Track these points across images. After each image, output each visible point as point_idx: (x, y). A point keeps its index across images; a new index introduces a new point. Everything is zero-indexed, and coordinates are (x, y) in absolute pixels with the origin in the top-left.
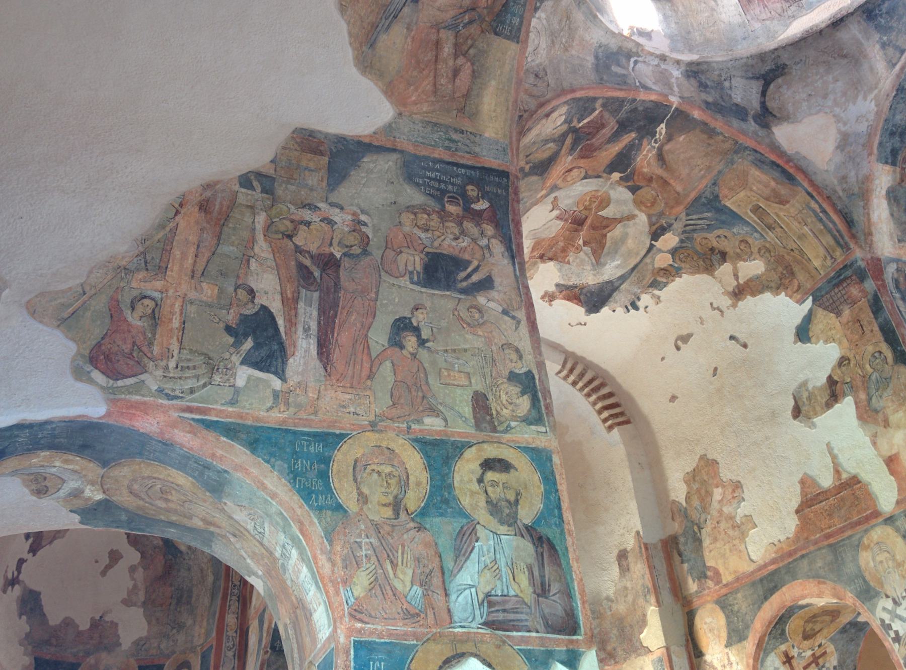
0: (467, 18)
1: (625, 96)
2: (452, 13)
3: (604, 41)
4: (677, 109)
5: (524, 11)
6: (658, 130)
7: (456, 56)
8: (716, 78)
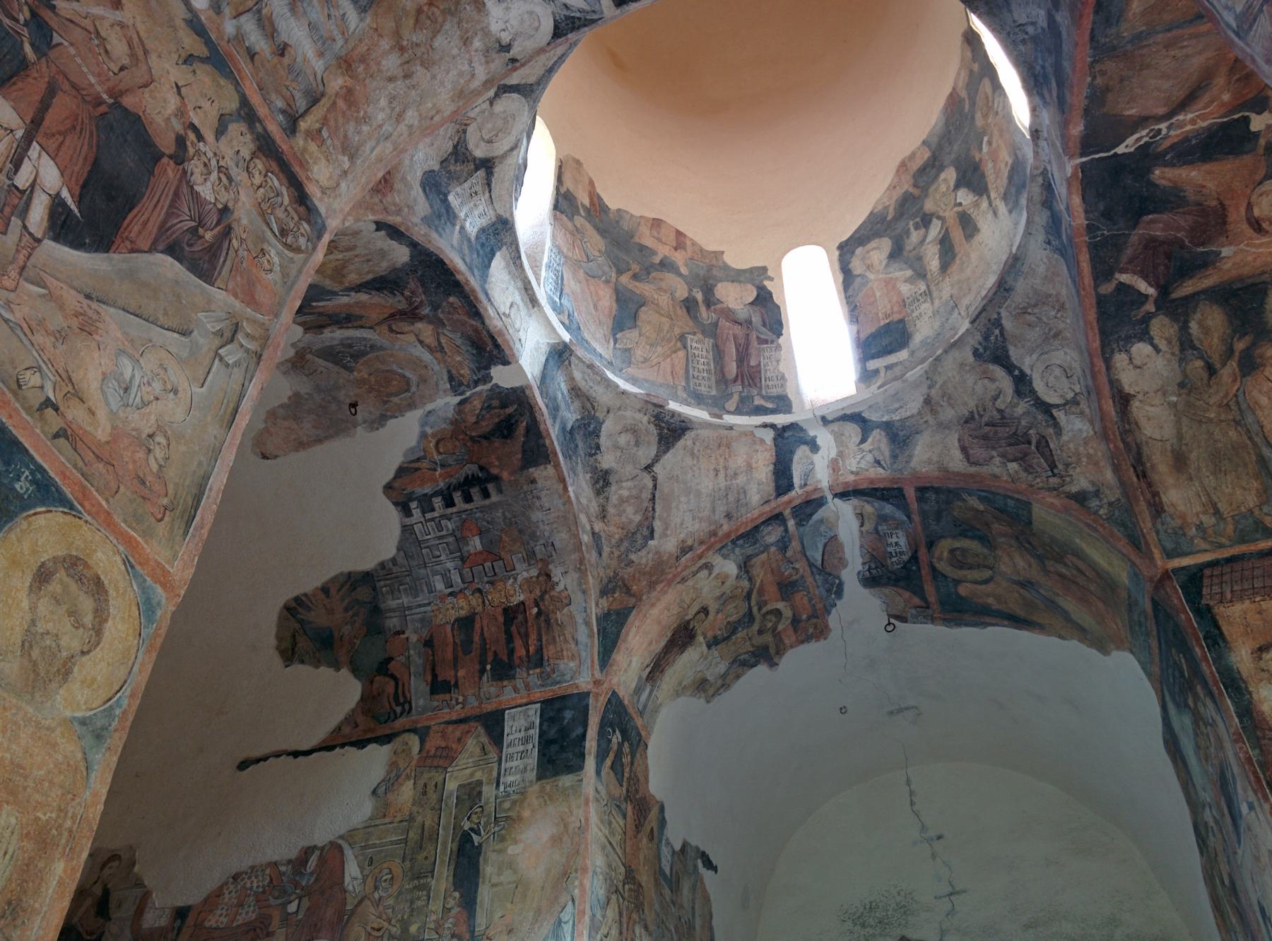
1: (1085, 249)
3: (1041, 237)
4: (1082, 155)
6: (1132, 149)
7: (1066, 565)
8: (1030, 45)
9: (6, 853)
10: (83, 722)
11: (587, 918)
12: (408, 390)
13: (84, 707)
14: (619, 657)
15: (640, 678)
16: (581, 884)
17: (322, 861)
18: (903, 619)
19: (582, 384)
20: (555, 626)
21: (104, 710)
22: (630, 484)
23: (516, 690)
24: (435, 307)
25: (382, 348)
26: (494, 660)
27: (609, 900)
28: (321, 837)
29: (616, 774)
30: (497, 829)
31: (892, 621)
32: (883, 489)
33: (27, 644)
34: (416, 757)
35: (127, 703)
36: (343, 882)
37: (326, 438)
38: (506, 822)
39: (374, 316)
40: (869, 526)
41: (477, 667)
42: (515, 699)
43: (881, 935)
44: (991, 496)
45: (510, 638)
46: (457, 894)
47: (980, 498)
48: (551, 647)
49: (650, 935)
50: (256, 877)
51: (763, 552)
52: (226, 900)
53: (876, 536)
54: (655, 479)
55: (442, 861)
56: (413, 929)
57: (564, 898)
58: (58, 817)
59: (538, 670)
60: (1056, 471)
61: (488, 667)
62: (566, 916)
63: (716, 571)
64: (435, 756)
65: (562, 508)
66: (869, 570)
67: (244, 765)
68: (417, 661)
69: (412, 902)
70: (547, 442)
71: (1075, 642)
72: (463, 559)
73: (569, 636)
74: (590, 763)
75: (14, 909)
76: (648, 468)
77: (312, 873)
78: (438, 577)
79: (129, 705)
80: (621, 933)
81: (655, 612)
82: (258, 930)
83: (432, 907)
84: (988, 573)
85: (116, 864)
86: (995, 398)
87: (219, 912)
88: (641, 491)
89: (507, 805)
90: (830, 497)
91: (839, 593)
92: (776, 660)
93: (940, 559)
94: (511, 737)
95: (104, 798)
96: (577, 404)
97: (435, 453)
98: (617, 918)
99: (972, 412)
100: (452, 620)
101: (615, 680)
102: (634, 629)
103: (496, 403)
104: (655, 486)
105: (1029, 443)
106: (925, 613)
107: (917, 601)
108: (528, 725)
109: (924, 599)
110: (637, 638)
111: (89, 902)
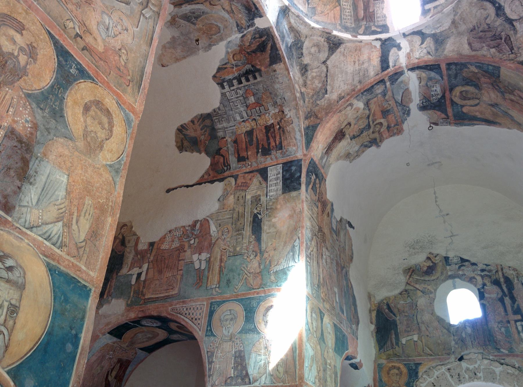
0: (497, 87)
2: (497, 92)
5: (485, 64)
7: (514, 95)
9: (89, 214)
10: (110, 166)
11: (304, 245)
12: (219, 32)
13: (110, 160)
14: (314, 144)
15: (322, 153)
16: (302, 232)
17: (201, 225)
18: (436, 124)
19: (294, 25)
20: (286, 133)
21: (118, 162)
22: (316, 70)
23: (272, 159)
25: (207, 13)
26: (262, 148)
27: (312, 238)
28: (200, 217)
29: (314, 191)
30: (267, 213)
31: (432, 125)
32: (431, 65)
33: (85, 136)
34: (234, 186)
35: (126, 159)
36: (210, 233)
37: (187, 56)
38: (271, 210)
40: (423, 83)
41: (256, 150)
42: (271, 163)
43: (421, 252)
44: (482, 65)
45: (268, 139)
46: (253, 237)
47: (476, 67)
48: (285, 141)
49: (329, 251)
50: (178, 231)
51: (375, 97)
52: (168, 240)
53: (426, 87)
54: (327, 67)
55: (247, 225)
56: (238, 249)
57: (294, 238)
58: (106, 201)
59: (280, 151)
60: (513, 51)
61: (260, 150)
62: (296, 244)
63: (354, 107)
64: (241, 186)
65: (288, 82)
66: (422, 103)
67: (168, 191)
68: (232, 149)
69: (237, 240)
70: (280, 53)
71: (515, 130)
72: (247, 106)
73: (292, 137)
74: (303, 187)
75: (95, 234)
76: (324, 62)
77: (198, 230)
78: (238, 114)
79: (126, 160)
80: (318, 250)
81: (328, 125)
82: (181, 250)
83: (244, 241)
84: (477, 101)
85: (125, 227)
86: (486, 18)
87: (165, 244)
88: (321, 73)
89: (271, 204)
90: (406, 70)
91: (408, 114)
92: (380, 144)
93: (455, 96)
94: (271, 178)
95: (122, 195)
96: (292, 34)
97: (233, 60)
98: (316, 245)
99: (474, 26)
100: (244, 132)
101: (312, 154)
102: (320, 133)
103: (257, 36)
104: (327, 71)
105: (501, 39)
106: (447, 120)
107: (443, 116)
108: (277, 173)
109: (447, 115)
110: (321, 136)
111: (118, 241)
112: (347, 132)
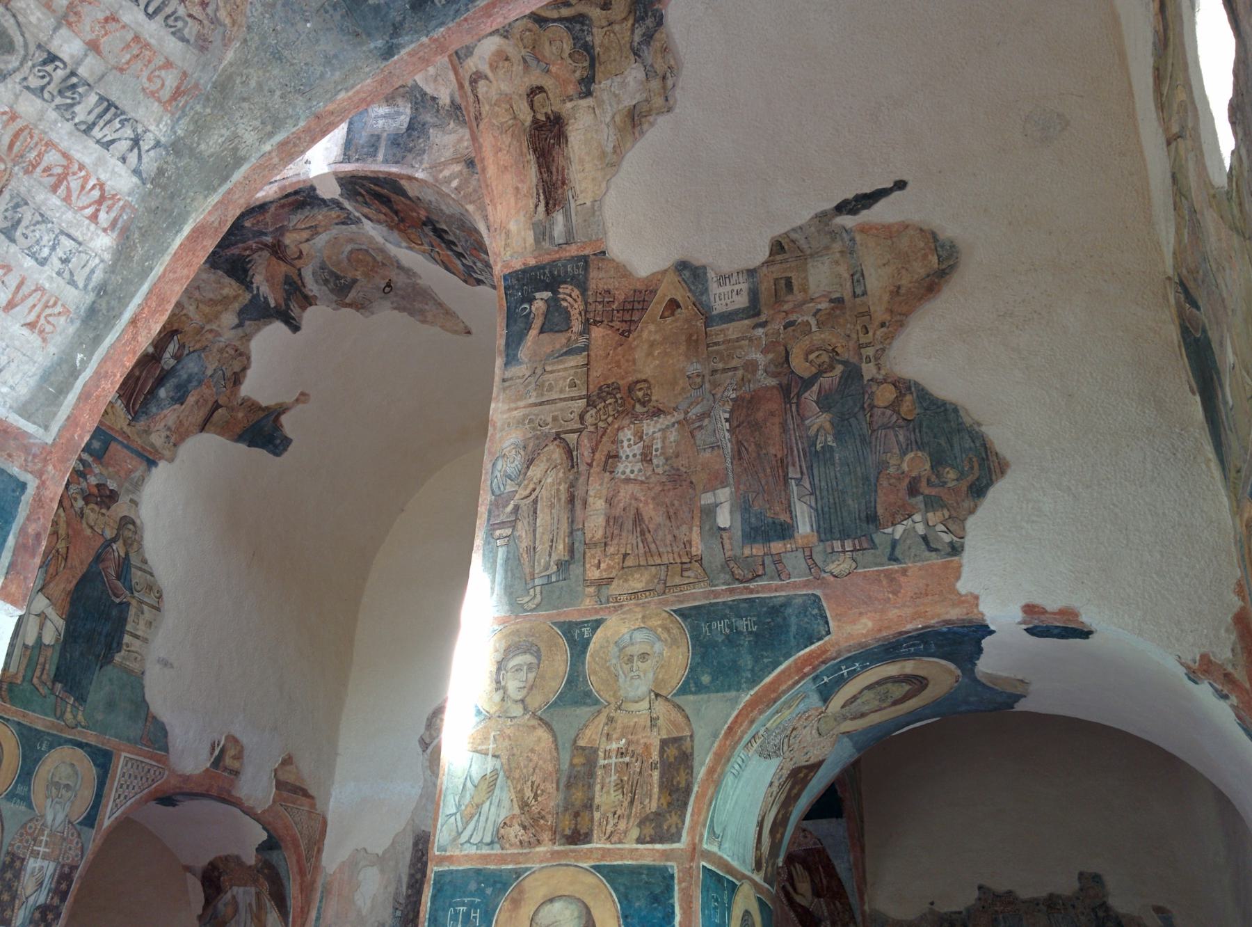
24: (263, 234)
25: (323, 262)
39: (283, 268)
63: (485, 68)
96: (400, 101)
103: (360, 199)
112: (555, 105)
